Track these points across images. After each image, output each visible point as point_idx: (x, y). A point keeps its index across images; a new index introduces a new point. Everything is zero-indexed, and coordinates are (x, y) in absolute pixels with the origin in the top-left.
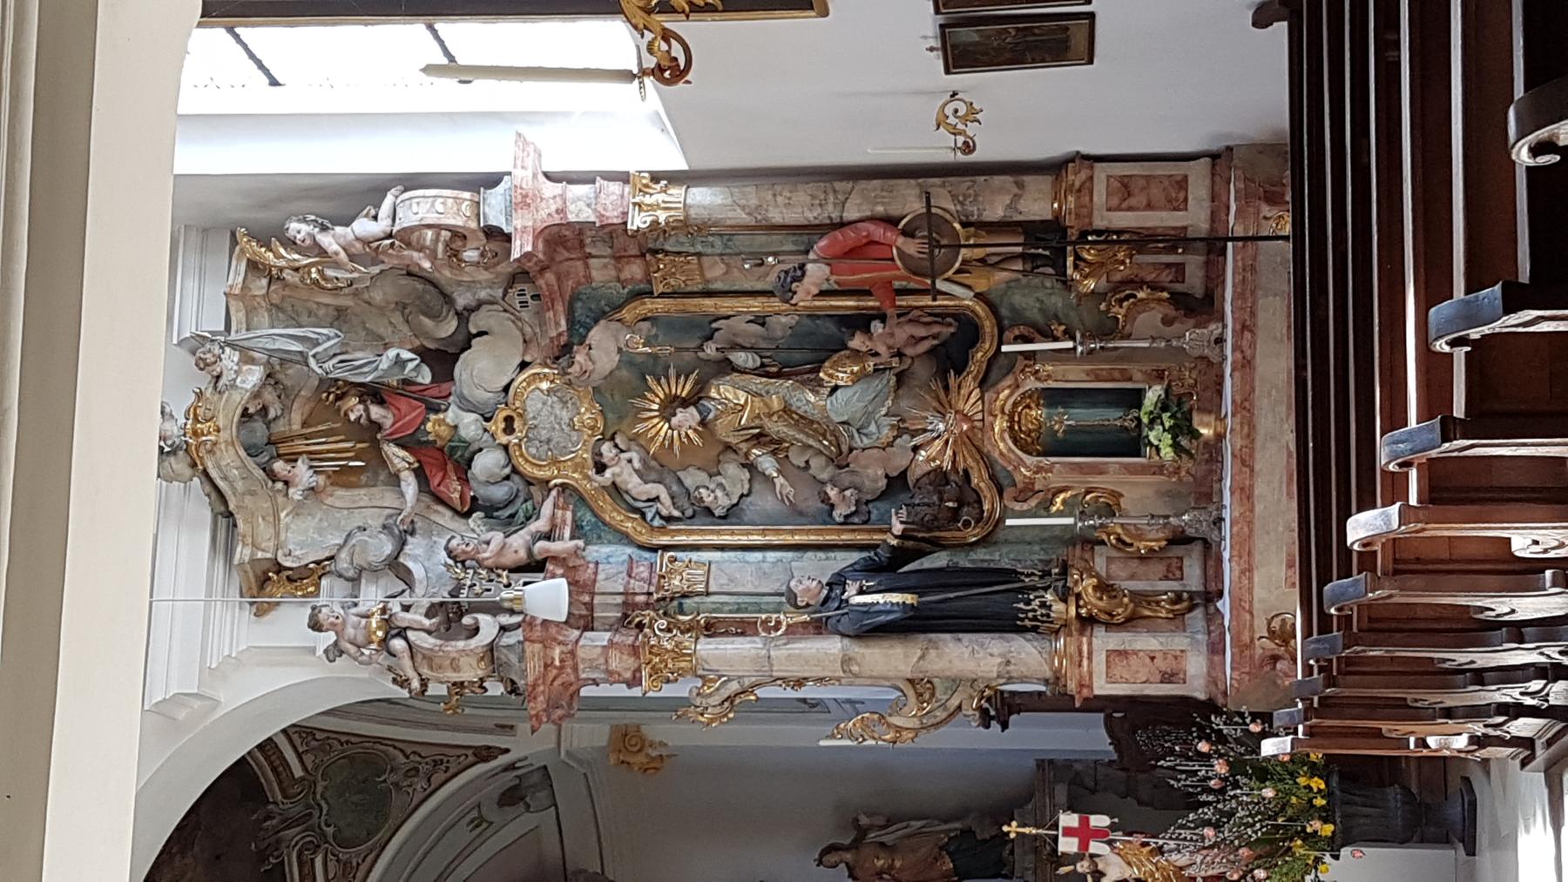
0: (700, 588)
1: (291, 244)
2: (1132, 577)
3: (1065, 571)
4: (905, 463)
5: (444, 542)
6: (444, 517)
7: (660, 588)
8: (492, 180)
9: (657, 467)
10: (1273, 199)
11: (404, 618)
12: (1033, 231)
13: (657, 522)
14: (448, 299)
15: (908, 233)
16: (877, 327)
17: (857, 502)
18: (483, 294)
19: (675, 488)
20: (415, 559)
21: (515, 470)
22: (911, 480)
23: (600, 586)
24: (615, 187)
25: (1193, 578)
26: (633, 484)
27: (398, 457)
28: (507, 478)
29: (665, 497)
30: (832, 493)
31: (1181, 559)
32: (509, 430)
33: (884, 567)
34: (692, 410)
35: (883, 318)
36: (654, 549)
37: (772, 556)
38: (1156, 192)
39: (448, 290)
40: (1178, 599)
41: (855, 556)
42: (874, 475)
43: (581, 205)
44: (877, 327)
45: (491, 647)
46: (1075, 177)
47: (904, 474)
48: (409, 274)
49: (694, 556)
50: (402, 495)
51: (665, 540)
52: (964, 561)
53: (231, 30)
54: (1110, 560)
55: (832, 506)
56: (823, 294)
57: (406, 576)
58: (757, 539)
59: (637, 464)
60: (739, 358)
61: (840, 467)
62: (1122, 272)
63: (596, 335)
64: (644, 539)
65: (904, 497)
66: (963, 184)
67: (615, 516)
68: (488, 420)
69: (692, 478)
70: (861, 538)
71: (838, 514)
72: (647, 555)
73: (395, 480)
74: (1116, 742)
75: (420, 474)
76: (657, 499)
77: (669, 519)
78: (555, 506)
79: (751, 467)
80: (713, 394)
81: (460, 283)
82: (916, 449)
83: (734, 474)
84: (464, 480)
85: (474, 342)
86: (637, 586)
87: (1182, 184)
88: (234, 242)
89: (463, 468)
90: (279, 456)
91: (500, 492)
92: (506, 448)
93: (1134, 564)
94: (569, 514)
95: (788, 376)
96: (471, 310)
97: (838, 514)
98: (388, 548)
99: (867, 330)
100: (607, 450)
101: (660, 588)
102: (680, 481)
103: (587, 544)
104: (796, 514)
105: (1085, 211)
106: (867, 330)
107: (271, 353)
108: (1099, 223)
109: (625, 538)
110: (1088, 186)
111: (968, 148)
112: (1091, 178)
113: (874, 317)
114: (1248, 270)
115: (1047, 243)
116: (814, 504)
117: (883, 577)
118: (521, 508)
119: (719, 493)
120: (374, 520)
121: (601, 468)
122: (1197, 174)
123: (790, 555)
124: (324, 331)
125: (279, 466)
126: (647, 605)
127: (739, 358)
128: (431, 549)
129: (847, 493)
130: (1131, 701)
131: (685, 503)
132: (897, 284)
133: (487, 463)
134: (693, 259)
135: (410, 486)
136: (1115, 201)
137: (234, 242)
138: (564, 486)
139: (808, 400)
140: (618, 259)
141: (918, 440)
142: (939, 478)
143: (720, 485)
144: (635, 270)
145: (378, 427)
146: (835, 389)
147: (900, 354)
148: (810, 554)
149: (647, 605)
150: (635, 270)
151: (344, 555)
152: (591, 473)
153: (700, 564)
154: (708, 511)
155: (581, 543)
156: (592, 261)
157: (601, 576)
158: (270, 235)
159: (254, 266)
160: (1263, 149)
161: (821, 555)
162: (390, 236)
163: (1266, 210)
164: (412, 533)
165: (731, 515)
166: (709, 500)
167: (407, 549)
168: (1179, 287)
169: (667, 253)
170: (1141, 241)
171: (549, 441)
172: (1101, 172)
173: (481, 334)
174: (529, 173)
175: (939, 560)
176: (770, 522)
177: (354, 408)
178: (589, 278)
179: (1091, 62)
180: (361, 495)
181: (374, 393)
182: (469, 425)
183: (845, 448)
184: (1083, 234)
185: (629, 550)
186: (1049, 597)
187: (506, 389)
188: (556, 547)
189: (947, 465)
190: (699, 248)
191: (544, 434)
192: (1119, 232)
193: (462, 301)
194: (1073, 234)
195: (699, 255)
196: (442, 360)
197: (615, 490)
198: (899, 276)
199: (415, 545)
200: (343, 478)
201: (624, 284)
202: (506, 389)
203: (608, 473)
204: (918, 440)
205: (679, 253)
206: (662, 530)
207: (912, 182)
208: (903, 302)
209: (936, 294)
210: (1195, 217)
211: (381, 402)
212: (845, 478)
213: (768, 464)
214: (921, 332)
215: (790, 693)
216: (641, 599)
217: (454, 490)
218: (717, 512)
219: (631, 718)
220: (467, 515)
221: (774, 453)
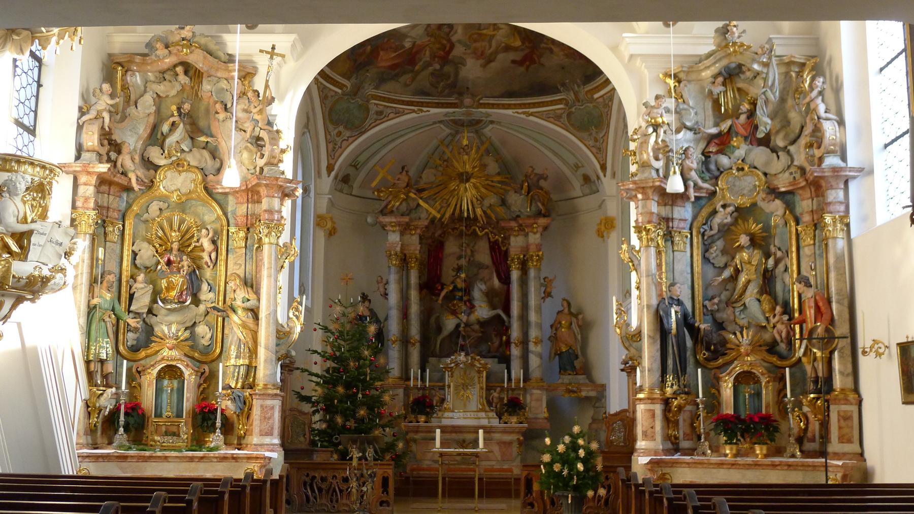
0: (676, 248)
1: (813, 79)
2: (684, 420)
3: (686, 393)
4: (729, 329)
5: (692, 145)
6: (702, 145)
7: (675, 232)
8: (844, 158)
9: (726, 231)
10: (845, 477)
11: (661, 131)
12: (829, 379)
13: (702, 230)
14: (793, 142)
15: (827, 330)
16: (786, 317)
17: (712, 311)
18: (795, 157)
19: (716, 237)
20: (685, 134)
21: (722, 172)
22: (723, 333)
23: (676, 209)
24: (842, 208)
25: (685, 444)
26: (717, 220)
27: (725, 126)
28: (718, 169)
29: (712, 233)
30: (716, 301)
31: (692, 440)
32: (739, 169)
33: (686, 321)
34: (749, 243)
35: (790, 319)
36: (691, 229)
37: (689, 276)
38: (846, 431)
39: (797, 143)
40: (676, 438)
41: (690, 309)
42: (725, 315)
43: (835, 195)
44: (786, 317)
45: (650, 166)
46: (852, 396)
47: (724, 329)
48: (802, 127)
49: (688, 246)
50: (709, 128)
51: (694, 233)
52: (689, 353)
53: (904, 50)
54: (691, 411)
55: (710, 300)
56: (800, 296)
57: (678, 131)
58: (696, 269)
59: (726, 221)
60: (771, 262)
61: (726, 303)
62: (811, 417)
63: (778, 202)
64: (695, 224)
65: (714, 330)
66: (848, 351)
67: (704, 213)
68: (742, 161)
69: (720, 244)
70: (697, 312)
71: (707, 303)
72: (688, 226)
73: (716, 125)
74: (616, 414)
75: (719, 135)
76: (711, 229)
77: (703, 235)
78: (707, 189)
79: (726, 266)
80: (756, 251)
81: (799, 147)
82: (735, 334)
83: (721, 261)
84: (717, 152)
85: (775, 155)
86: (676, 223)
87: (850, 441)
88: (813, 57)
89: (721, 152)
90: (725, 79)
91: (713, 167)
92: (731, 168)
93: (688, 421)
94: (704, 195)
95: (764, 281)
96: (788, 152)
97: (707, 303)
98: (688, 124)
99: (784, 313)
100: (730, 209)
101: (675, 232)
102: (719, 239)
103: (693, 203)
104: (706, 287)
105: (837, 401)
106: (784, 313)
107: (767, 74)
108: (832, 407)
109: (695, 218)
110: (847, 401)
111: (864, 353)
112: (851, 404)
113: (790, 316)
114: (814, 467)
115: (825, 385)
116: (711, 293)
117: (682, 321)
118: (707, 176)
119: (714, 255)
120: (700, 118)
121: (724, 206)
122: (854, 448)
123: (690, 284)
124: (777, 94)
125: (720, 79)
126: (668, 227)
127: (771, 262)
128: (690, 141)
129: (716, 307)
130: (633, 421)
131: (709, 241)
132: (804, 325)
133: (724, 160)
134: (812, 242)
135: (714, 131)
136: (842, 414)
137: (813, 57)
138: (714, 193)
139: (753, 290)
140: (812, 211)
141: (738, 334)
142: (724, 342)
143: (717, 256)
144: (806, 218)
145: (738, 118)
146: (759, 301)
147: (774, 327)
148: (690, 292)
149: (668, 227)
150: (806, 218)
151: (685, 106)
152: (721, 203)
153: (685, 247)
154: (706, 251)
155: (693, 199)
156: (810, 200)
157: (679, 208)
158: (818, 70)
159: (803, 65)
160: (866, 473)
161: (690, 296)
162: (819, 118)
163: (839, 476)
164: (695, 133)
165: (706, 259)
166: (712, 251)
167: (688, 132)
168: (805, 440)
169: (815, 231)
170: (825, 425)
171: (734, 186)
172: (854, 408)
173: (778, 157)
174: (848, 173)
175: (689, 343)
176: (704, 275)
177: (745, 107)
178: (803, 200)
179: (903, 403)
180: (710, 112)
181: (752, 114)
182: (740, 152)
183: (735, 305)
184: (827, 401)
185: (690, 219)
186: (675, 387)
187: (755, 168)
188: (691, 190)
189: (729, 346)
190: (817, 244)
191: (737, 183)
192: (828, 415)
193: (792, 148)
194: (828, 397)
195: (814, 244)
196: (765, 142)
197: (714, 212)
198: (809, 325)
199: (689, 135)
200: (716, 104)
201: (802, 214)
202: (755, 168)
203: (721, 209)
204: (738, 334)
205: (815, 236)
206: (699, 232)
207: (848, 331)
208: (797, 328)
209: (801, 339)
210: (834, 446)
211: (748, 118)
212: (723, 305)
213: (726, 274)
214: (784, 335)
215: (634, 285)
216: (671, 224)
217: (713, 149)
218: (707, 255)
219: (618, 224)
220: (703, 154)
221: (732, 276)
